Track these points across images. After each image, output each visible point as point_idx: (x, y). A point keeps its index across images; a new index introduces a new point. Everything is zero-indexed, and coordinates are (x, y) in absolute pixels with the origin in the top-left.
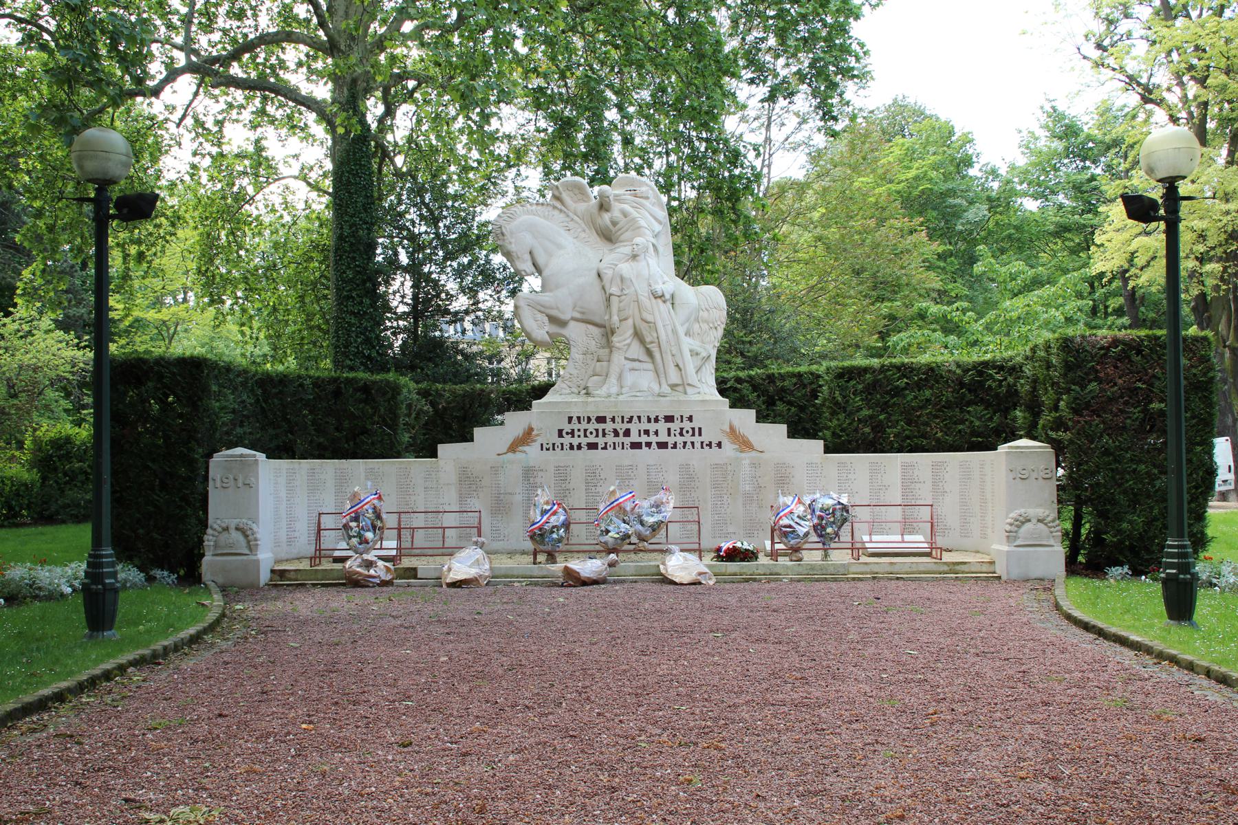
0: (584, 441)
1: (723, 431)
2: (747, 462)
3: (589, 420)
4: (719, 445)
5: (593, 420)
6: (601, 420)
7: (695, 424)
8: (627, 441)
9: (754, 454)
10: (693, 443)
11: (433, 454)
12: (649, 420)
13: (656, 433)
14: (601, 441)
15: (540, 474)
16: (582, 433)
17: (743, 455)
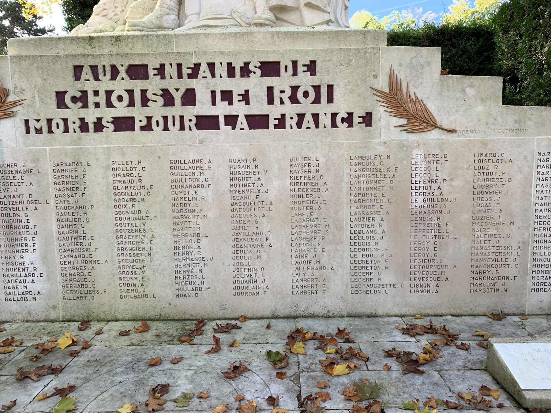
0: (108, 114)
1: (377, 92)
2: (419, 152)
3: (115, 72)
4: (367, 119)
5: (123, 73)
6: (138, 71)
7: (322, 78)
8: (190, 112)
9: (434, 135)
10: (316, 117)
11: (88, 123)
12: (231, 72)
13: (246, 97)
14: (139, 114)
15: (27, 178)
16: (102, 99)
17: (413, 137)
